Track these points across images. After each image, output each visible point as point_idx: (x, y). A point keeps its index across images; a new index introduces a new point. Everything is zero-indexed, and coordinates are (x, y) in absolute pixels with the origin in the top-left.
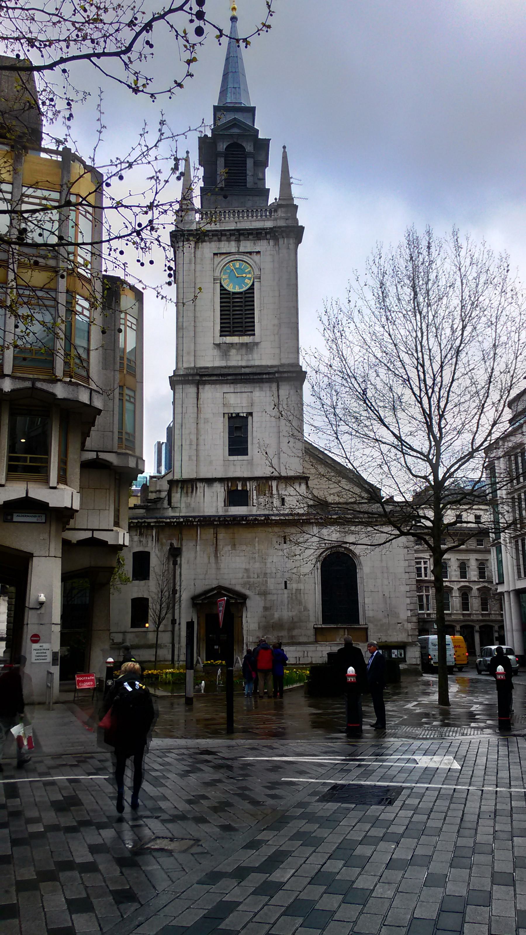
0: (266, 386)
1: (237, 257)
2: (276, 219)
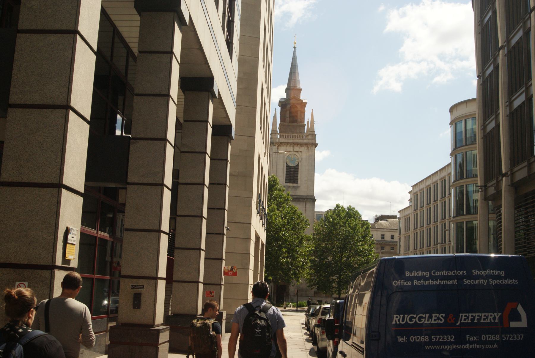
0: (301, 203)
1: (293, 153)
2: (308, 139)
